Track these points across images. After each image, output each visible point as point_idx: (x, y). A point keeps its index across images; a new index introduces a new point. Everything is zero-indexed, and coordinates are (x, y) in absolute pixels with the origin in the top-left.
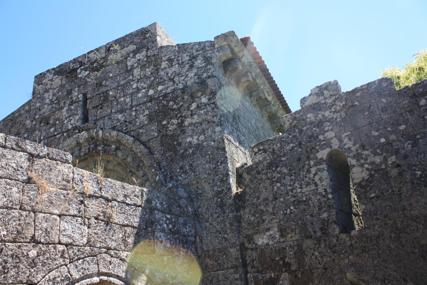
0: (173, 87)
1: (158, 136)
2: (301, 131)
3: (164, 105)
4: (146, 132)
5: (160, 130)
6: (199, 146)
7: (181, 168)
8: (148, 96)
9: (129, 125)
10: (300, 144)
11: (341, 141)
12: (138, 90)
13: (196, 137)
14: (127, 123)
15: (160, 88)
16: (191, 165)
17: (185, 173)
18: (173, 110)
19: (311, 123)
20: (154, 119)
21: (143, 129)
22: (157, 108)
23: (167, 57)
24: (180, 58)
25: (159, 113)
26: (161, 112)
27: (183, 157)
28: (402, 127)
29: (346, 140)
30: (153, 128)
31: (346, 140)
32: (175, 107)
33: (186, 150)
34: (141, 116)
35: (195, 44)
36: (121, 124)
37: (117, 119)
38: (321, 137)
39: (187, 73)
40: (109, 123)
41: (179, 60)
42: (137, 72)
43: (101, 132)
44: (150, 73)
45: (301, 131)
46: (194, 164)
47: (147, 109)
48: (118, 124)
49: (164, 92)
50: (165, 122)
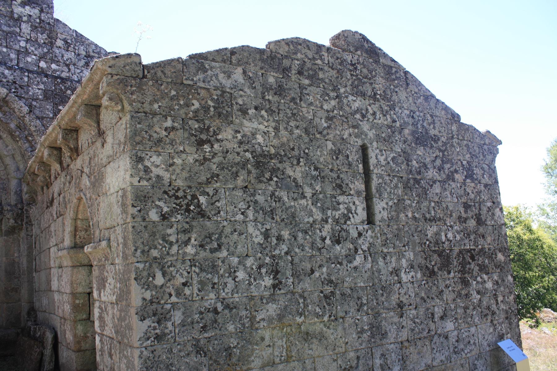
0: (68, 75)
3: (61, 90)
4: (40, 108)
5: (55, 113)
8: (39, 66)
9: (20, 89)
12: (27, 53)
14: (18, 87)
15: (54, 66)
20: (50, 99)
21: (37, 103)
22: (53, 88)
23: (64, 37)
24: (77, 48)
25: (56, 94)
26: (59, 95)
30: (48, 107)
34: (34, 87)
35: (92, 43)
36: (8, 82)
39: (83, 69)
41: (76, 50)
42: (26, 28)
44: (42, 41)
47: (43, 83)
48: (4, 80)
49: (58, 73)
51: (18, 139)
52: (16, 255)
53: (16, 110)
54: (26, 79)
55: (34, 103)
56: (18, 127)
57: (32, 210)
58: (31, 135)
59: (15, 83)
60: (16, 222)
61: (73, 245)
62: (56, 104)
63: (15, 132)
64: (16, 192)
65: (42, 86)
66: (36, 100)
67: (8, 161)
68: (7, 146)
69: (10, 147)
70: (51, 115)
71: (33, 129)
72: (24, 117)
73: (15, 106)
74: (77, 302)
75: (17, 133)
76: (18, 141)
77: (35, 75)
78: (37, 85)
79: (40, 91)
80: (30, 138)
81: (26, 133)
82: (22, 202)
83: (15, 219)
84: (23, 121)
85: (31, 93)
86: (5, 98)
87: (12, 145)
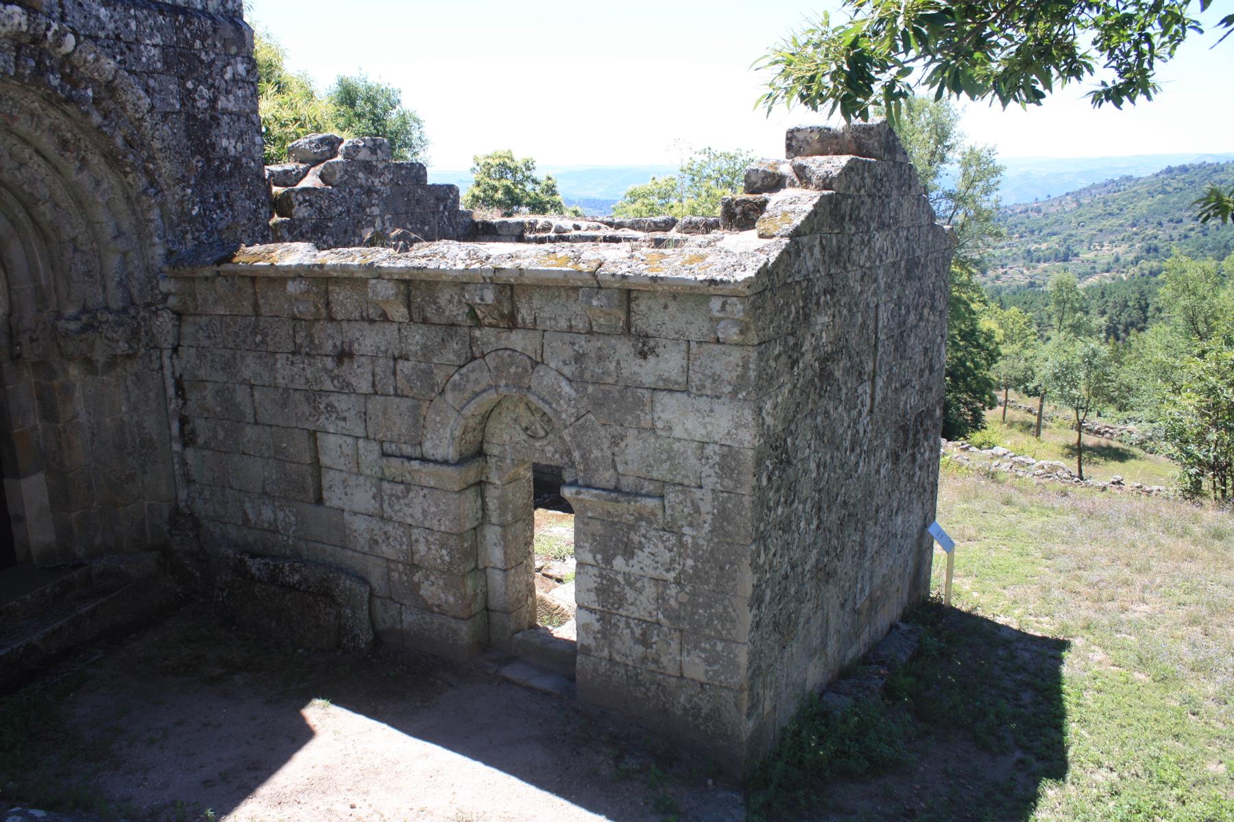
1: (179, 113)
2: (351, 193)
6: (236, 161)
7: (216, 197)
10: (349, 211)
11: (383, 223)
13: (233, 142)
16: (228, 196)
17: (221, 207)
18: (202, 62)
19: (361, 187)
27: (219, 176)
28: (426, 228)
29: (387, 224)
31: (387, 224)
32: (203, 56)
33: (222, 164)
36: (107, 37)
37: (98, 18)
38: (368, 210)
40: (77, 16)
43: (70, 40)
45: (351, 193)
46: (232, 196)
48: (102, 34)
50: (190, 85)
51: (128, 169)
52: (124, 409)
53: (129, 106)
54: (133, 25)
55: (152, 83)
56: (129, 143)
57: (161, 319)
58: (151, 158)
59: (118, 37)
60: (130, 347)
61: (457, 458)
62: (182, 78)
63: (125, 157)
64: (120, 283)
65: (158, 40)
66: (150, 74)
67: (101, 215)
68: (98, 183)
69: (105, 186)
70: (178, 106)
71: (157, 144)
72: (142, 119)
73: (129, 97)
74: (466, 545)
75: (131, 158)
76: (126, 174)
77: (145, 12)
78: (151, 36)
79: (154, 51)
80: (151, 166)
81: (145, 154)
82: (133, 304)
83: (128, 342)
84: (139, 128)
85: (144, 59)
86: (112, 82)
87: (110, 180)
